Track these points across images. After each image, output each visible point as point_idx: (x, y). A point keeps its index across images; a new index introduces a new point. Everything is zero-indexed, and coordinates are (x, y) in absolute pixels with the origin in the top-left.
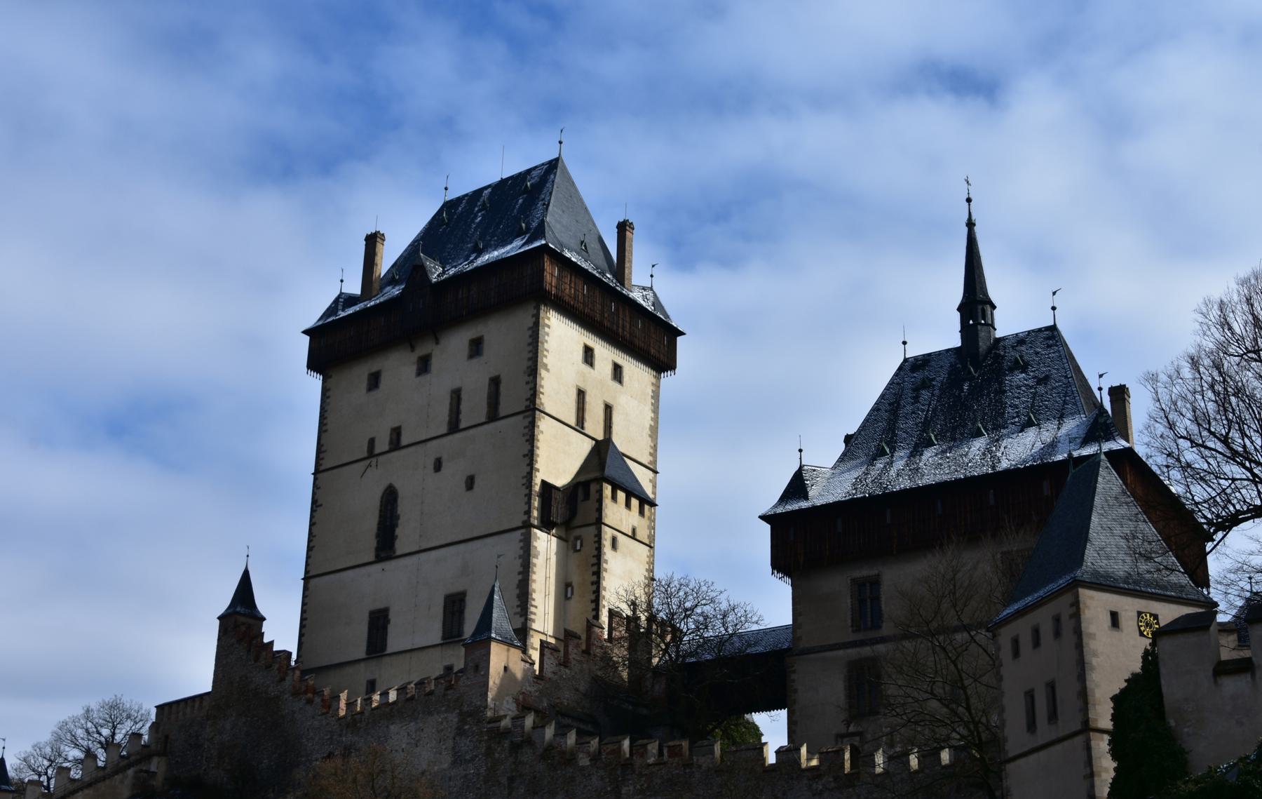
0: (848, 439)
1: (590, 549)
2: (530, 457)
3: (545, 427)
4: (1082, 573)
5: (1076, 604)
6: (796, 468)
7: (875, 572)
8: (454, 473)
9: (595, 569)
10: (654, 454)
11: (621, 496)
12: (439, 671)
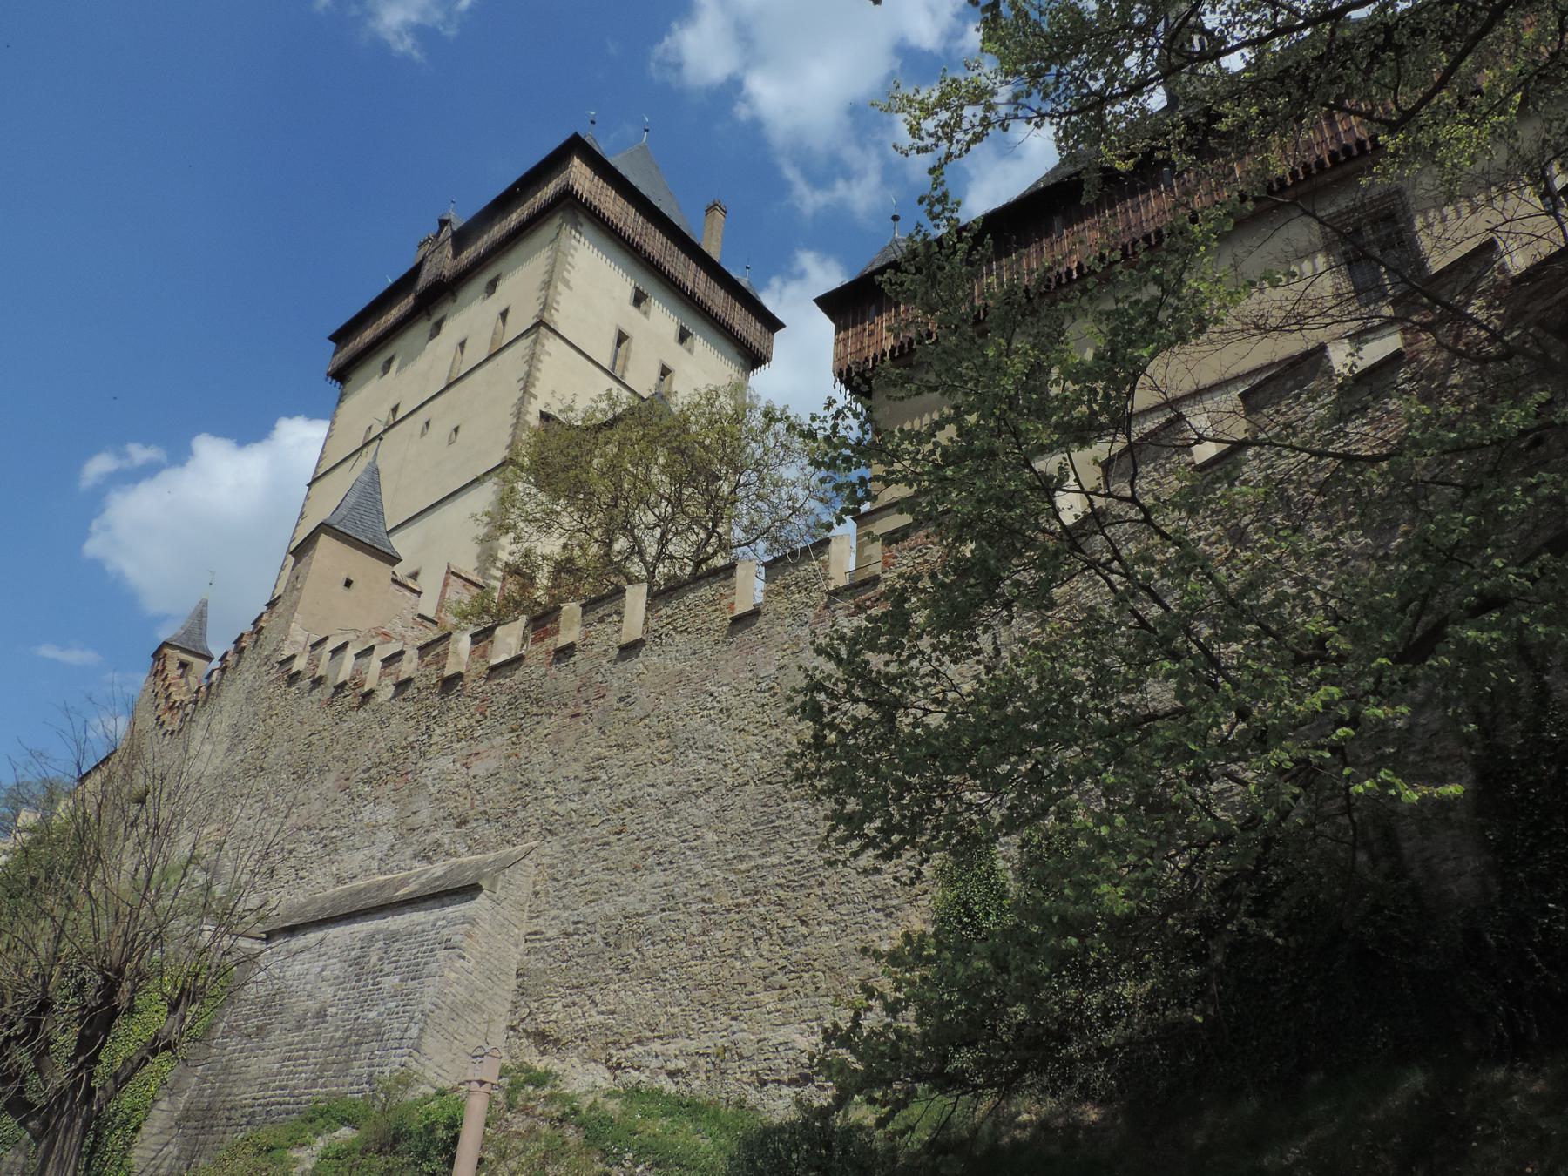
2: (527, 383)
8: (440, 430)
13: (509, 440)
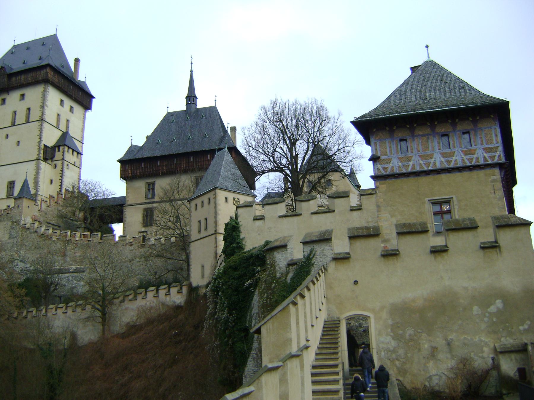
0: (147, 137)
1: (59, 167)
2: (40, 136)
3: (45, 125)
4: (218, 185)
5: (215, 194)
6: (130, 145)
7: (153, 181)
8: (13, 139)
9: (61, 175)
10: (83, 137)
11: (71, 151)
12: (5, 207)
13: (38, 153)
